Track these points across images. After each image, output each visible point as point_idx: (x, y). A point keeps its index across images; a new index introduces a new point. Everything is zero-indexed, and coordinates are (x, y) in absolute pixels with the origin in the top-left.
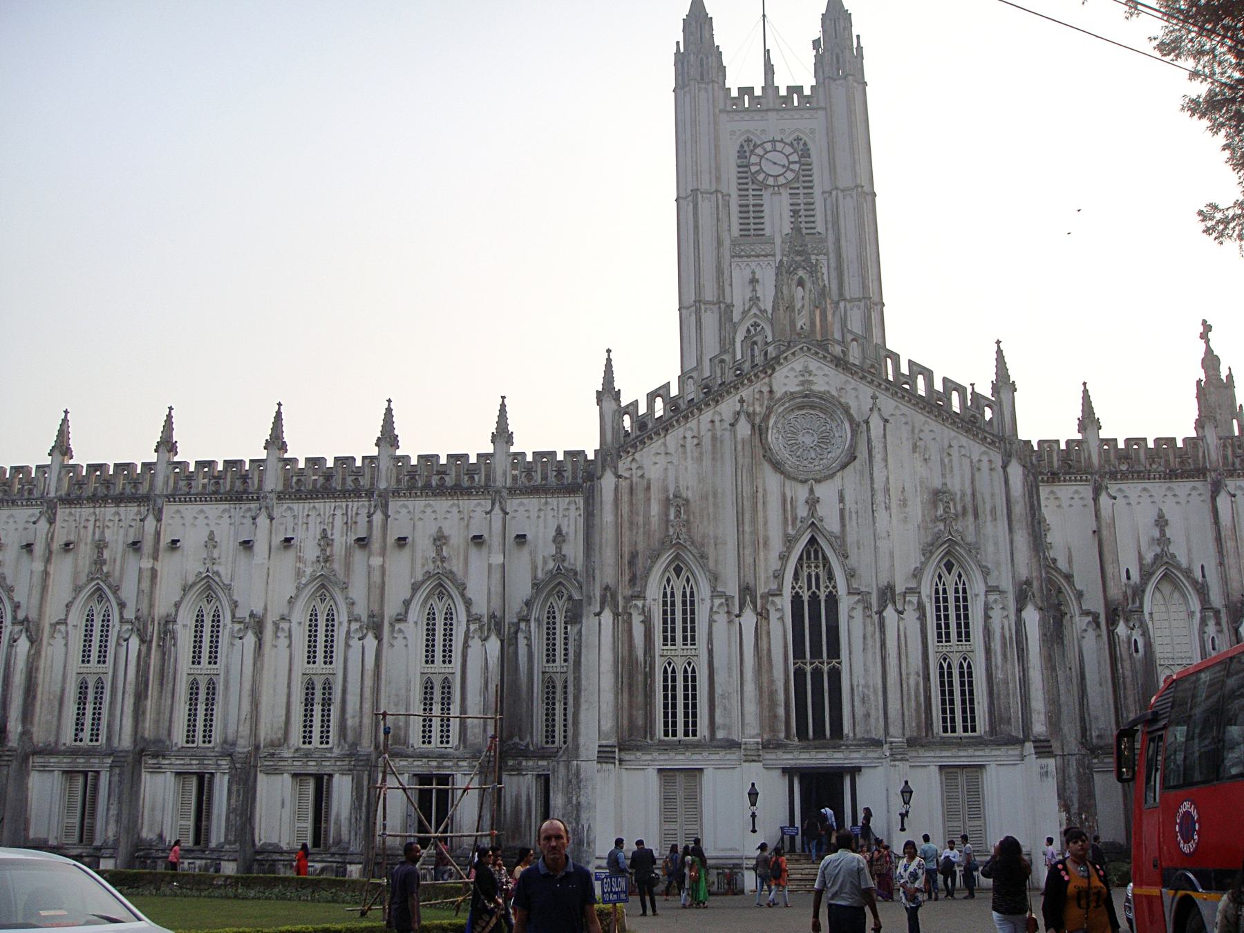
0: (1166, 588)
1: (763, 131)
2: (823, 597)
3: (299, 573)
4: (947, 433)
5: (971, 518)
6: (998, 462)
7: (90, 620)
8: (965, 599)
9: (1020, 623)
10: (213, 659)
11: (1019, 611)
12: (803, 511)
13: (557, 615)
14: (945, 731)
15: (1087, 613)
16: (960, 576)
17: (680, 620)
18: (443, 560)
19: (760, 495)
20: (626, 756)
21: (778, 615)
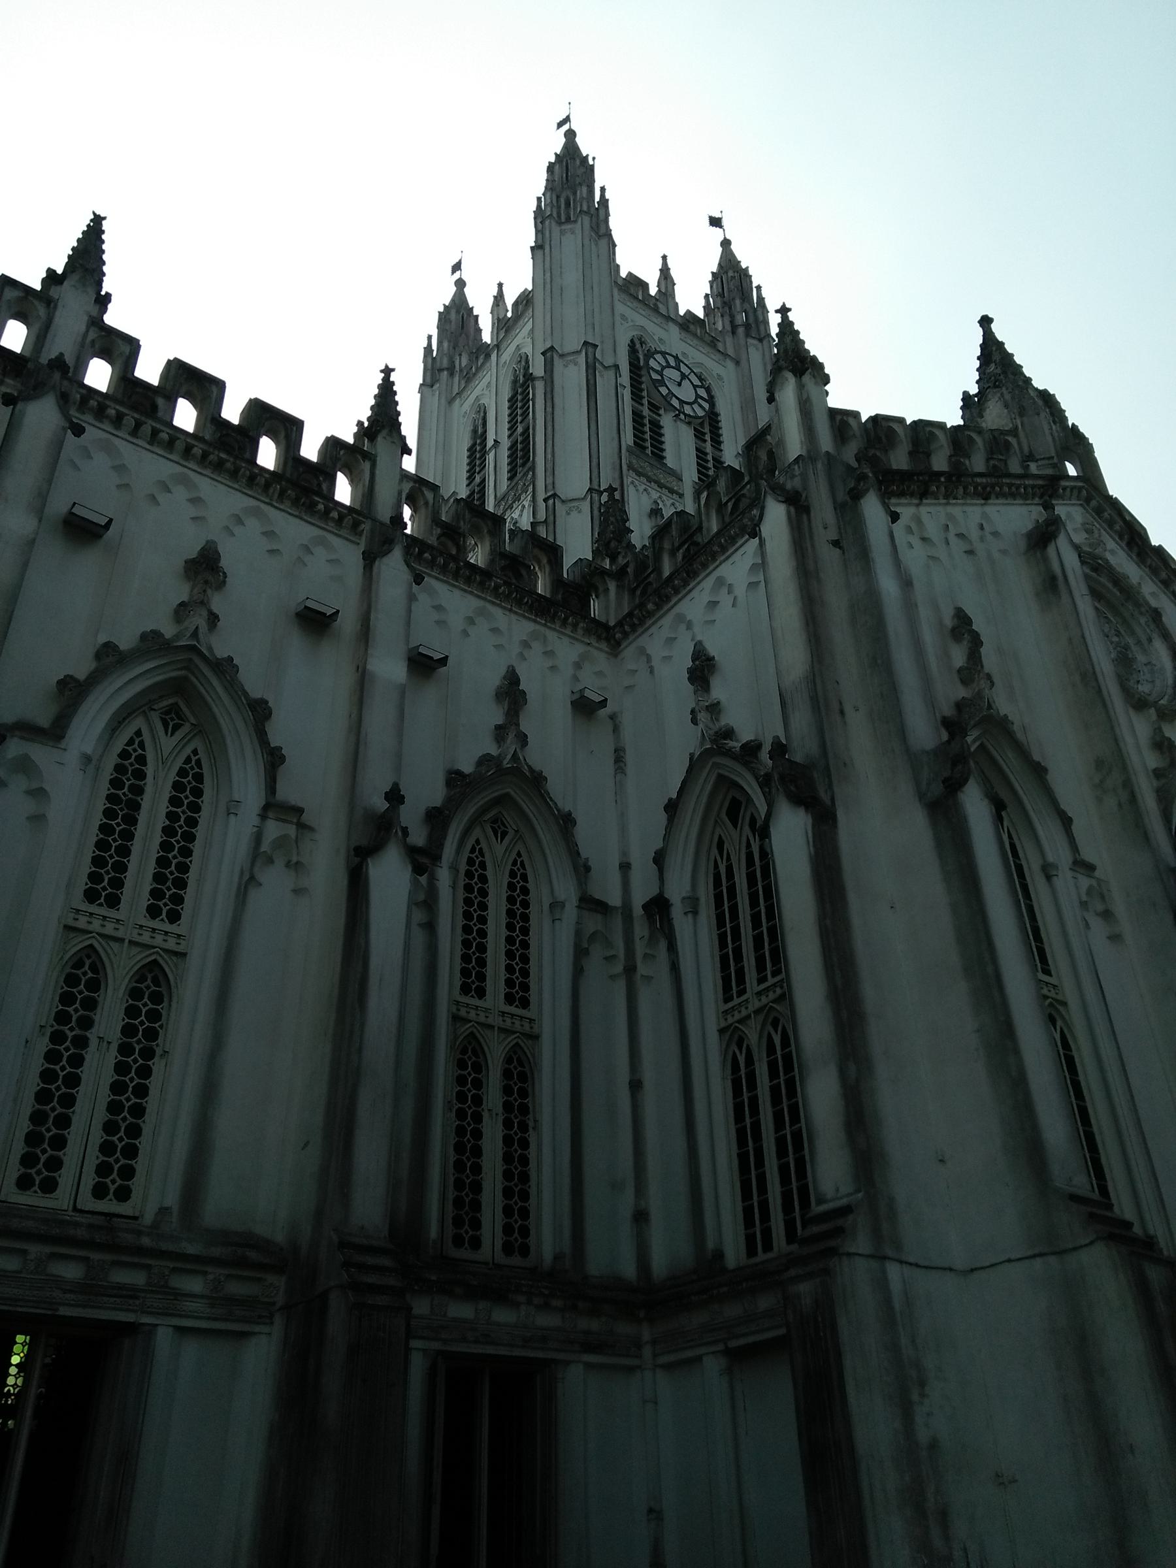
13: (489, 873)
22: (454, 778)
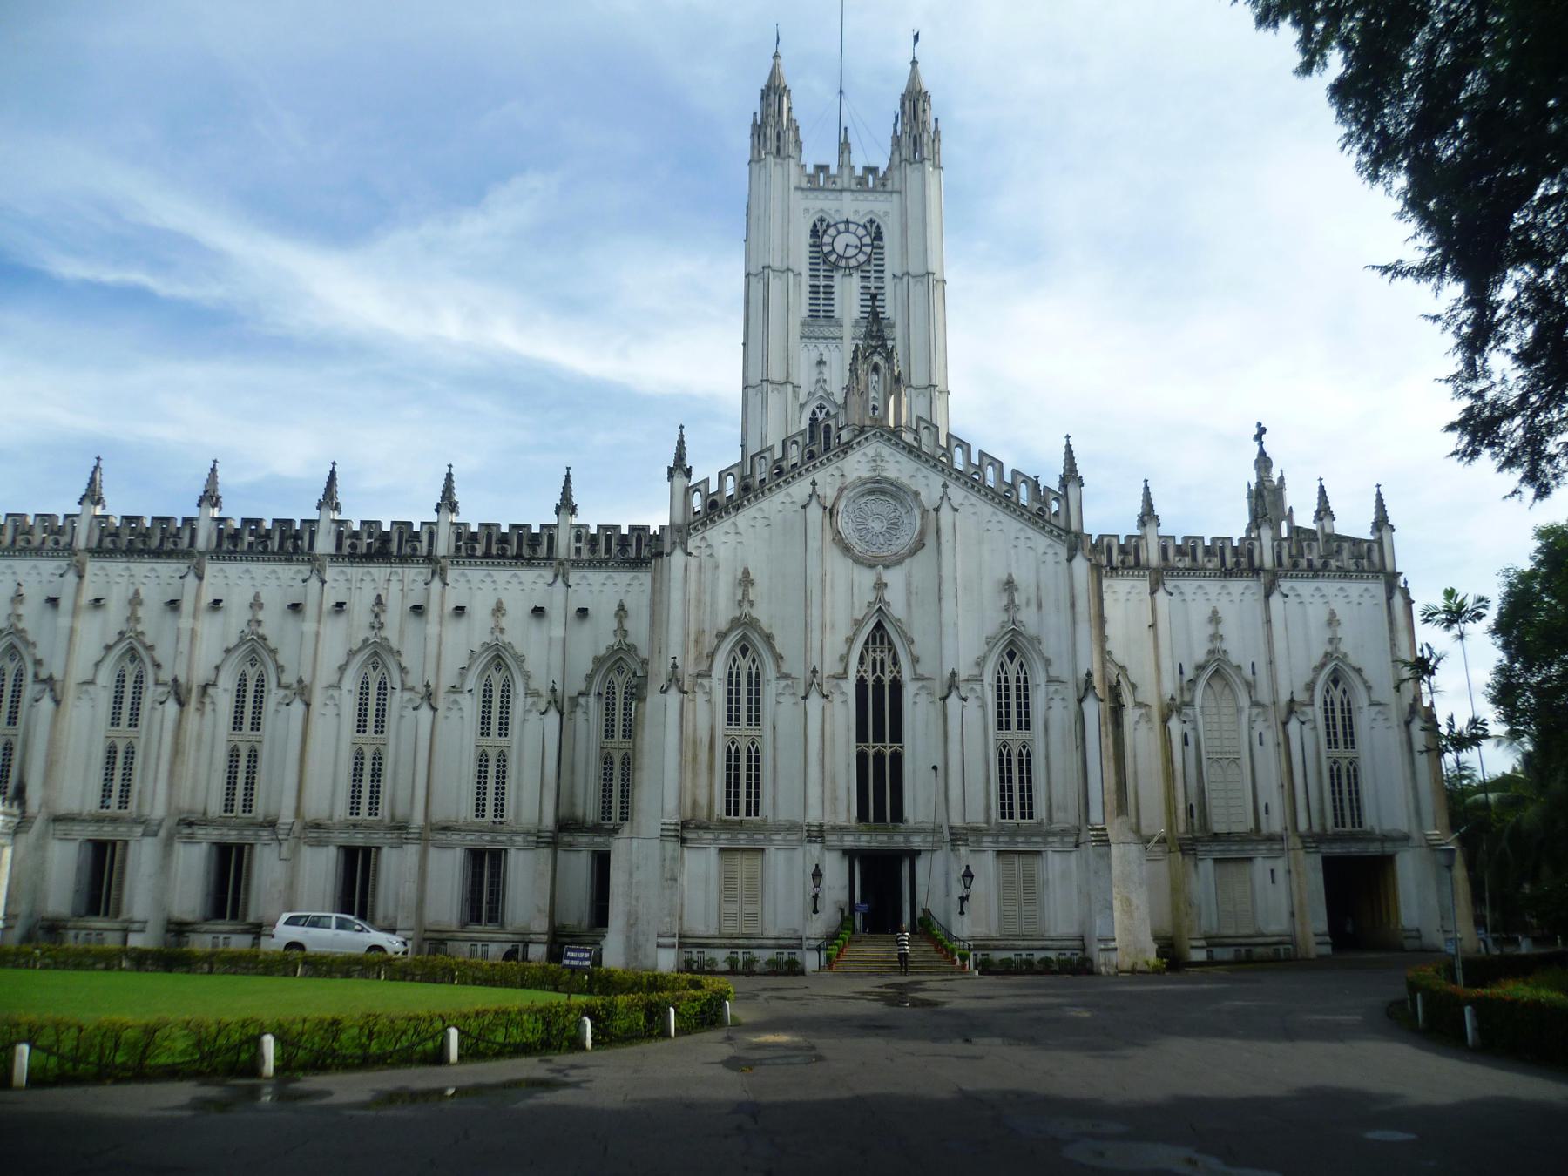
0: (1217, 685)
1: (837, 211)
2: (887, 680)
4: (1012, 525)
5: (1034, 608)
6: (1063, 553)
7: (121, 680)
8: (1026, 688)
9: (1081, 718)
10: (256, 726)
11: (1080, 701)
14: (1003, 816)
15: (1138, 705)
16: (1022, 665)
17: (745, 702)
18: (502, 631)
19: (828, 578)
20: (689, 835)
21: (842, 698)
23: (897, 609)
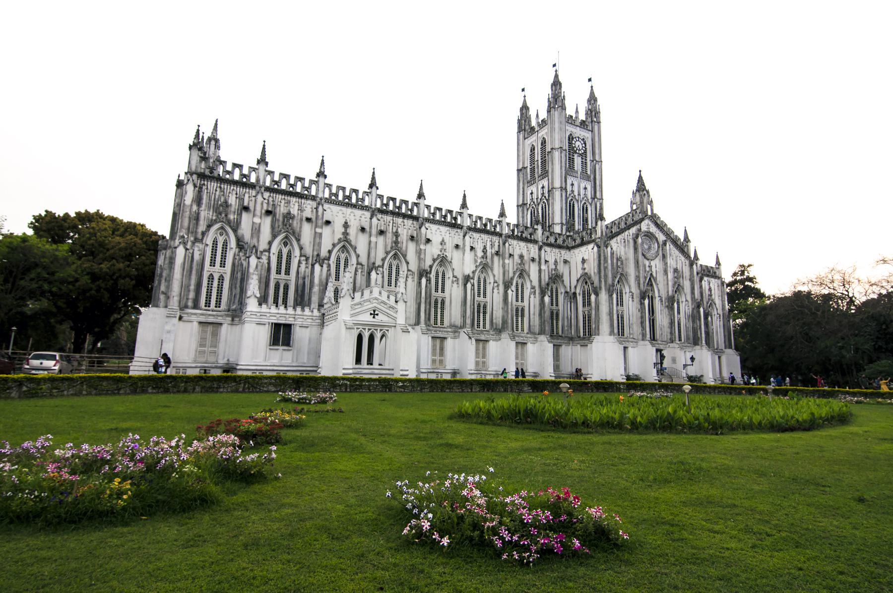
3: (476, 261)
12: (648, 269)
22: (549, 278)
23: (654, 274)
